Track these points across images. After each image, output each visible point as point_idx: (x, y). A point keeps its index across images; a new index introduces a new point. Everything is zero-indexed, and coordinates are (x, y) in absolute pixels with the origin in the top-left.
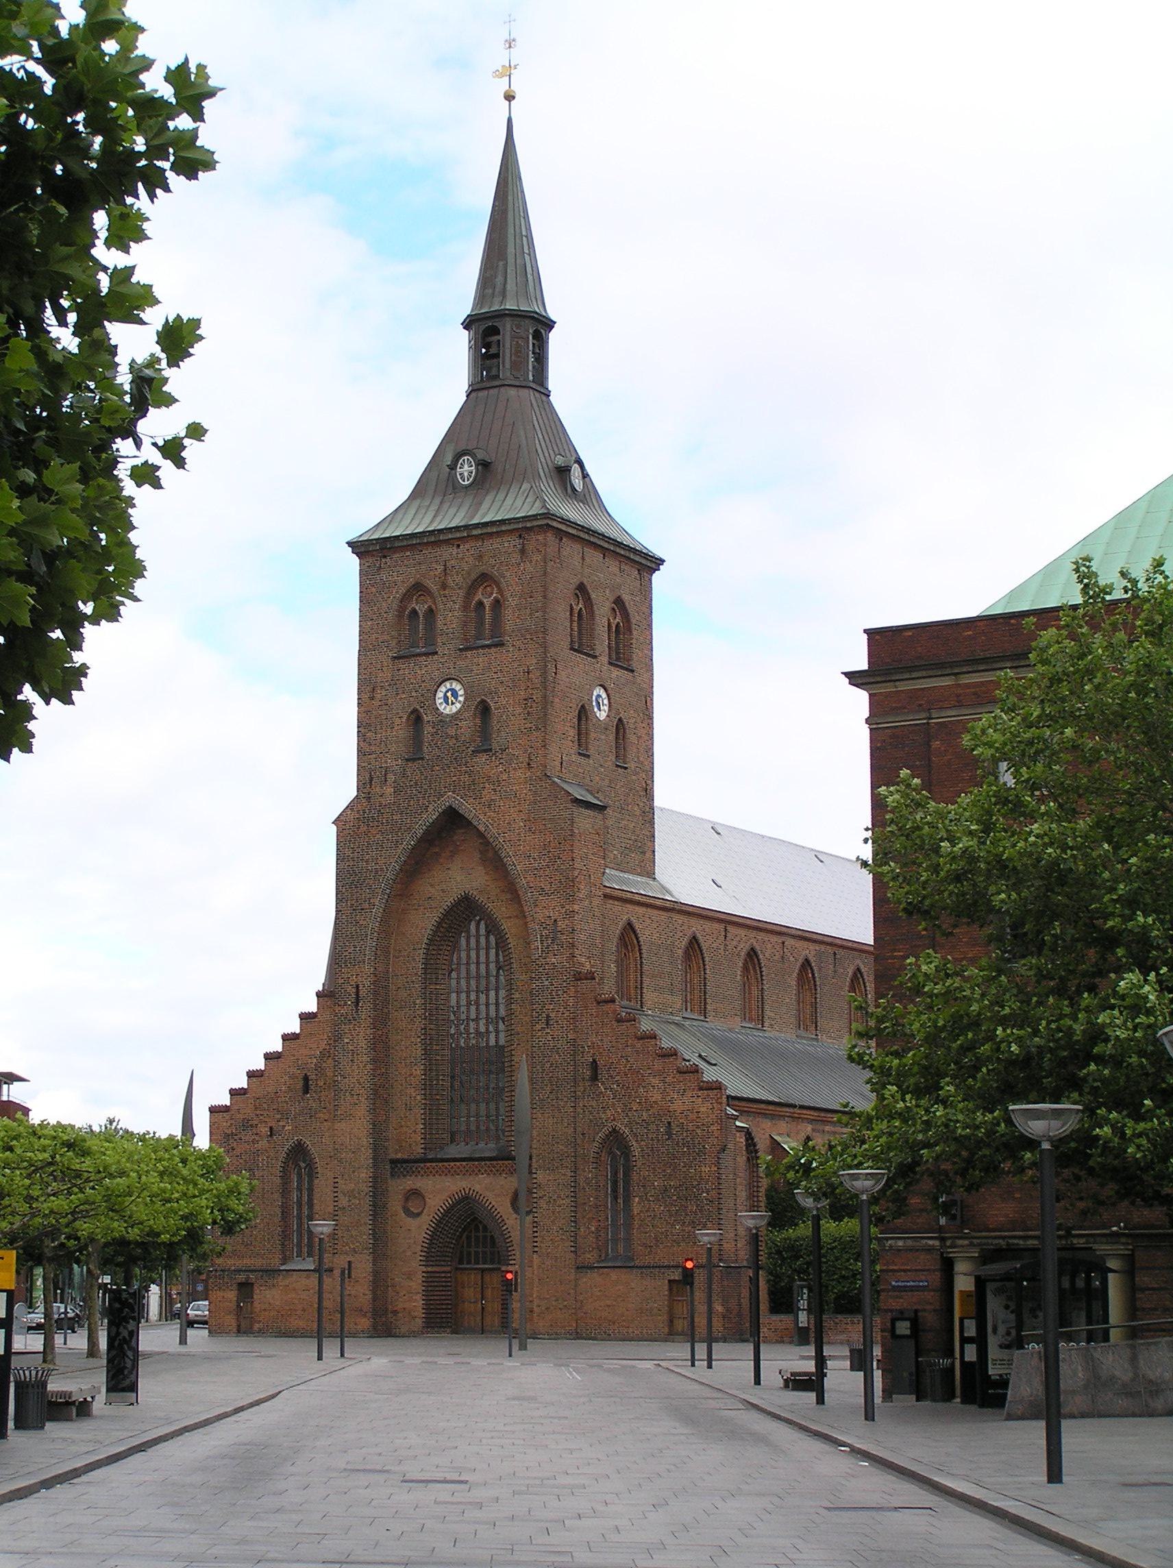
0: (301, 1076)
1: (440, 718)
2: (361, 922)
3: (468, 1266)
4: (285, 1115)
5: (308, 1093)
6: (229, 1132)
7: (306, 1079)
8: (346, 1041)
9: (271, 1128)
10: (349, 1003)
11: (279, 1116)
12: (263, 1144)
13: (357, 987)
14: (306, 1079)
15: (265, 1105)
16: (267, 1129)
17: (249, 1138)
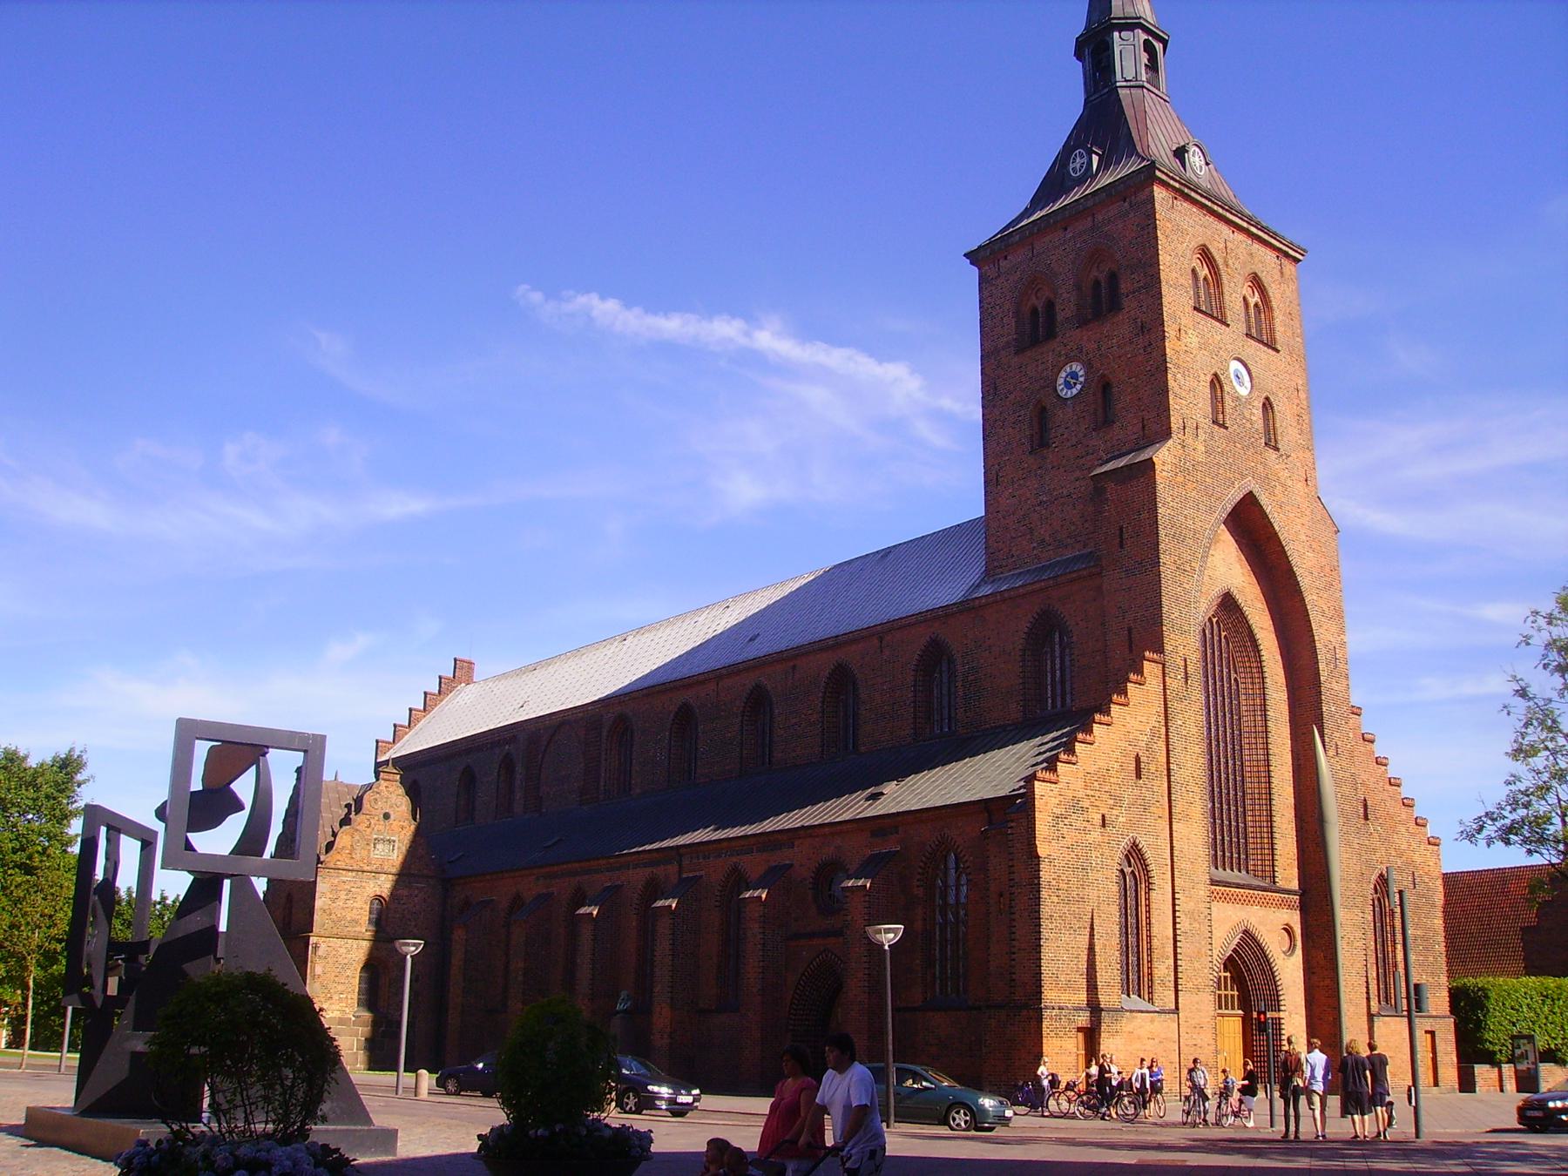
0: (1134, 755)
1: (1236, 395)
2: (1185, 585)
3: (1226, 1012)
4: (1118, 801)
5: (1141, 778)
6: (1058, 811)
7: (1138, 760)
8: (1180, 722)
9: (1103, 816)
10: (1179, 677)
11: (1112, 802)
12: (1096, 835)
13: (1185, 660)
14: (1138, 760)
15: (1096, 784)
16: (1100, 817)
17: (1080, 824)
